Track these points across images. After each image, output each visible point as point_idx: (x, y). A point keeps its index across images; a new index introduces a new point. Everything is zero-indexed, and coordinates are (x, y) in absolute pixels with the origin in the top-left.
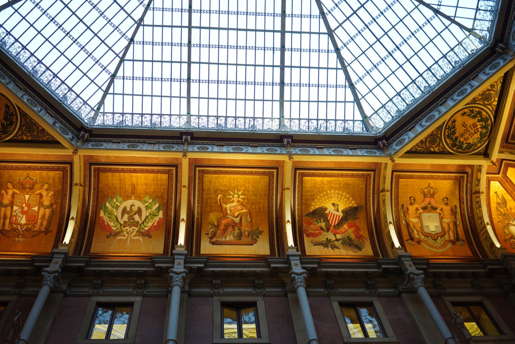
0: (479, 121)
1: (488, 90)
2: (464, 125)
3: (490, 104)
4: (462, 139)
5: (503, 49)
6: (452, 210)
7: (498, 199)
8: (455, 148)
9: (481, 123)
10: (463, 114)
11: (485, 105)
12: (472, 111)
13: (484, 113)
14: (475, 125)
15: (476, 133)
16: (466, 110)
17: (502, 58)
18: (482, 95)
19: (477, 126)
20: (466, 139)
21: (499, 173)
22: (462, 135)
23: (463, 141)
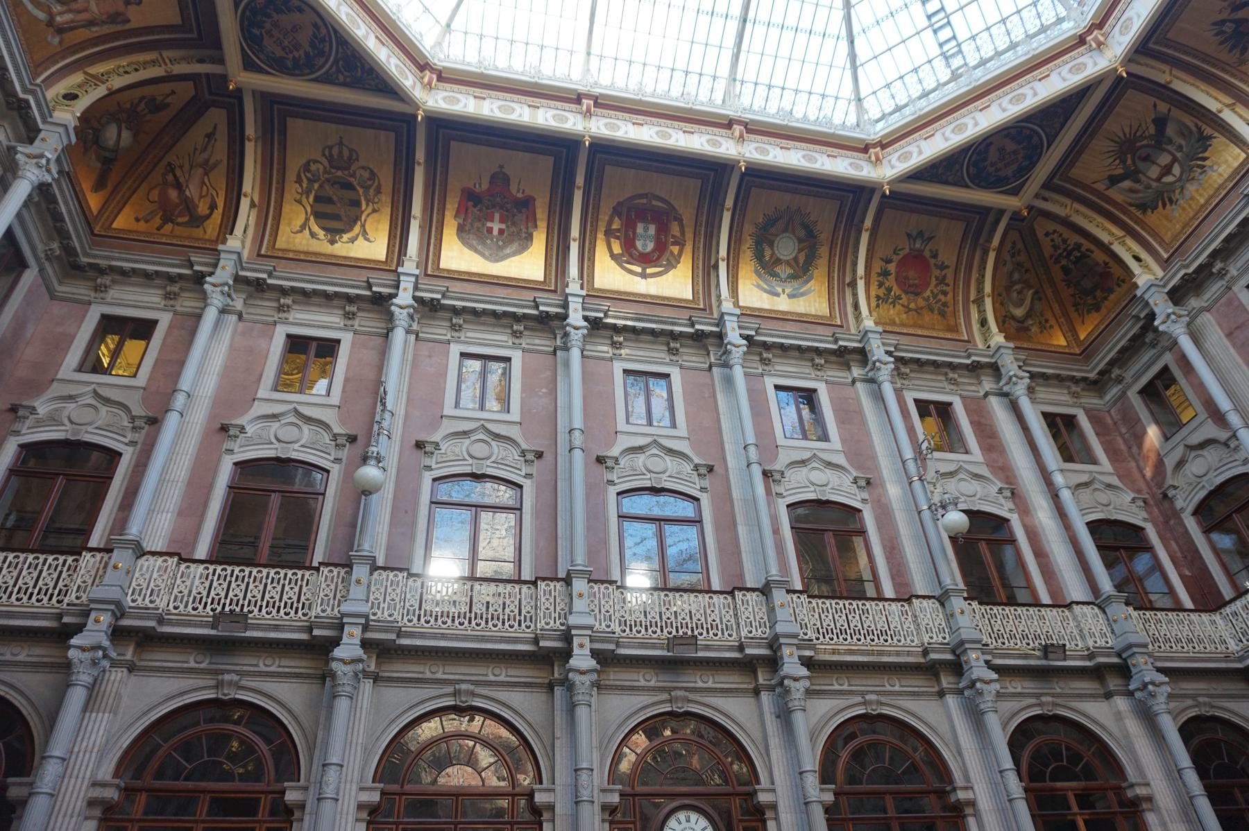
0: (307, 54)
1: (363, 65)
2: (295, 28)
3: (338, 71)
4: (268, 25)
5: (430, 83)
6: (118, 14)
7: (162, 98)
8: (248, 13)
9: (303, 56)
10: (315, 25)
11: (336, 61)
12: (323, 40)
13: (322, 60)
14: (297, 47)
15: (284, 49)
16: (323, 30)
17: (415, 83)
18: (354, 57)
19: (297, 50)
20: (268, 32)
21: (211, 93)
22: (276, 25)
23: (263, 28)
